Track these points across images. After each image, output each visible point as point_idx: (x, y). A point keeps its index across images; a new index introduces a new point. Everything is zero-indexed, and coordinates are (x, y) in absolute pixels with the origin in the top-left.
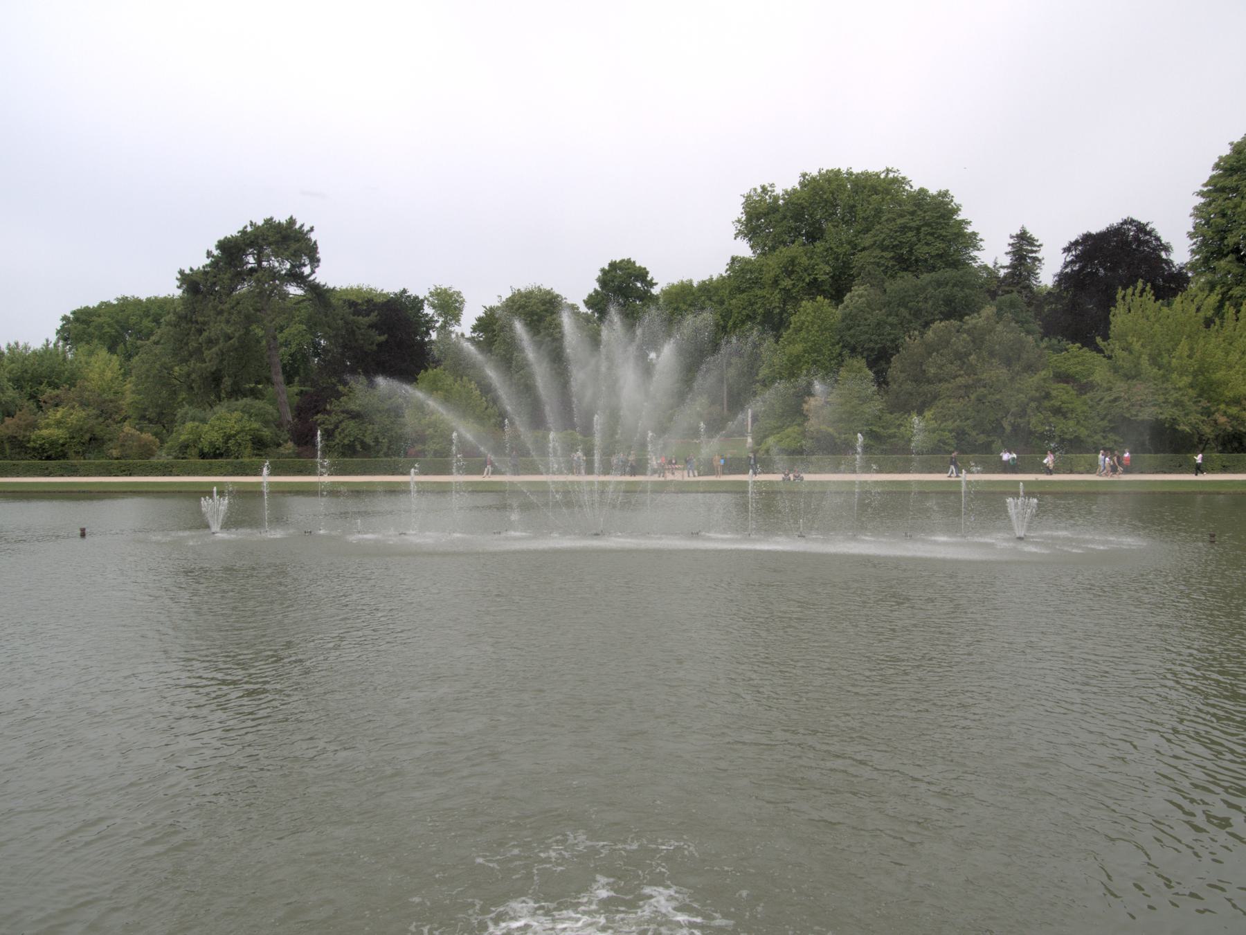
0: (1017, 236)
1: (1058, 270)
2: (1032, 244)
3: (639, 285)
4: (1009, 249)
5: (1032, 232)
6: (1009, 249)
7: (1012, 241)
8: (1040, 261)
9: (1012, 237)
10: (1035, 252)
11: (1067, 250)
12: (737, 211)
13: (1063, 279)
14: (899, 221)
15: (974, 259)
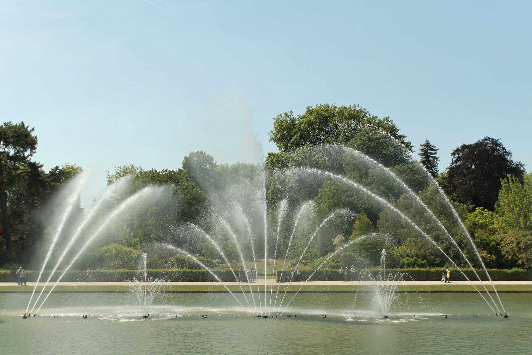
0: (424, 145)
1: (449, 166)
2: (432, 150)
3: (208, 166)
4: (420, 152)
5: (432, 143)
6: (420, 152)
7: (421, 148)
8: (437, 159)
9: (421, 146)
10: (434, 154)
11: (453, 154)
12: (271, 126)
13: (452, 171)
14: (367, 135)
15: (410, 157)
